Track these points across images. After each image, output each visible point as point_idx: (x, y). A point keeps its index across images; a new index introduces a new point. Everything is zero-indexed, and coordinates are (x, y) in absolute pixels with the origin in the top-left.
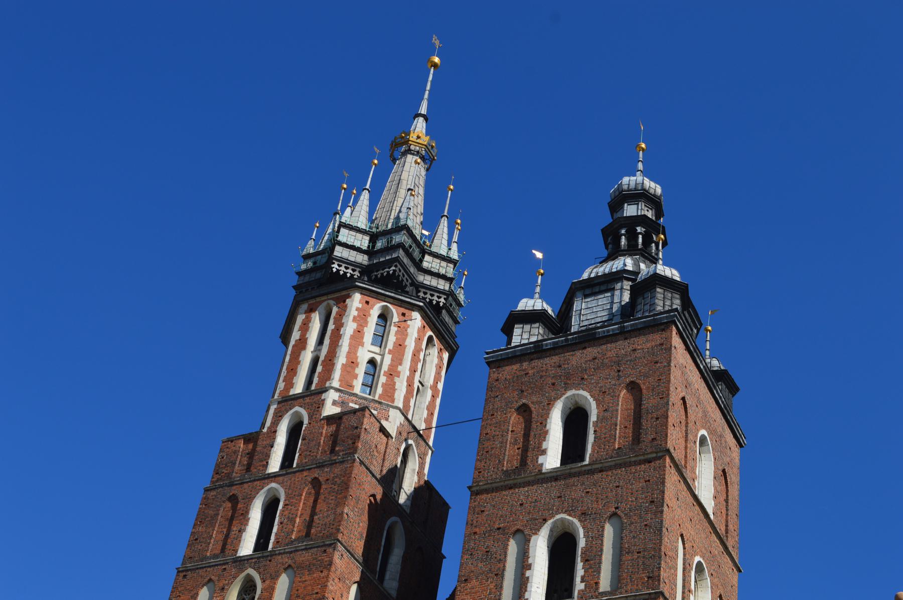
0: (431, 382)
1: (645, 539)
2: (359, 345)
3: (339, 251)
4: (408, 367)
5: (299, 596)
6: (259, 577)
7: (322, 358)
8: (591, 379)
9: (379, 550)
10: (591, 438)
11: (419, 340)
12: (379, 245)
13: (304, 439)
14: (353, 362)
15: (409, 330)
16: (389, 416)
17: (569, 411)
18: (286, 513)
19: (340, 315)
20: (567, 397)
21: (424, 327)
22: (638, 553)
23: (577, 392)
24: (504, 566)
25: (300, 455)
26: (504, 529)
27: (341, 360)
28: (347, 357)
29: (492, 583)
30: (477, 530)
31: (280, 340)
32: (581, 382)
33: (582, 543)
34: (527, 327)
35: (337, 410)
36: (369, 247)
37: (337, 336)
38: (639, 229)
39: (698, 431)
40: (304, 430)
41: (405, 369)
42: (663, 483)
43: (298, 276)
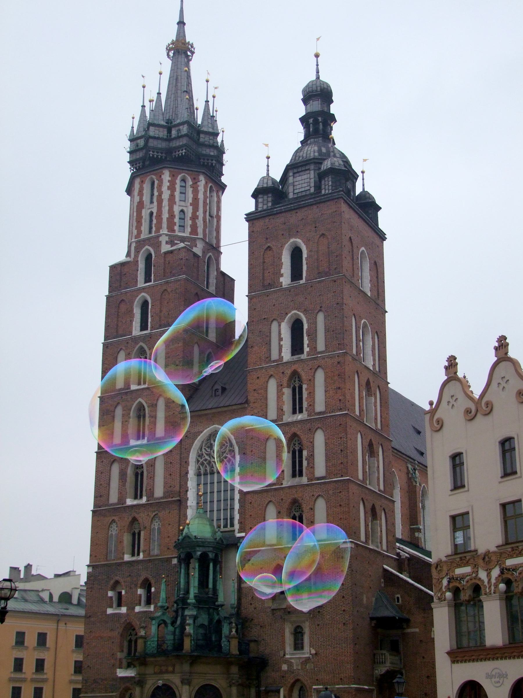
0: (215, 213)
1: (336, 324)
3: (152, 143)
4: (202, 212)
7: (155, 214)
11: (205, 192)
12: (174, 132)
13: (154, 266)
14: (172, 216)
15: (199, 188)
19: (160, 186)
21: (207, 182)
22: (333, 331)
23: (295, 240)
26: (267, 318)
27: (165, 215)
32: (297, 234)
33: (306, 326)
34: (265, 197)
36: (167, 136)
37: (160, 201)
38: (320, 119)
39: (359, 250)
41: (200, 213)
42: (342, 293)
43: (129, 154)
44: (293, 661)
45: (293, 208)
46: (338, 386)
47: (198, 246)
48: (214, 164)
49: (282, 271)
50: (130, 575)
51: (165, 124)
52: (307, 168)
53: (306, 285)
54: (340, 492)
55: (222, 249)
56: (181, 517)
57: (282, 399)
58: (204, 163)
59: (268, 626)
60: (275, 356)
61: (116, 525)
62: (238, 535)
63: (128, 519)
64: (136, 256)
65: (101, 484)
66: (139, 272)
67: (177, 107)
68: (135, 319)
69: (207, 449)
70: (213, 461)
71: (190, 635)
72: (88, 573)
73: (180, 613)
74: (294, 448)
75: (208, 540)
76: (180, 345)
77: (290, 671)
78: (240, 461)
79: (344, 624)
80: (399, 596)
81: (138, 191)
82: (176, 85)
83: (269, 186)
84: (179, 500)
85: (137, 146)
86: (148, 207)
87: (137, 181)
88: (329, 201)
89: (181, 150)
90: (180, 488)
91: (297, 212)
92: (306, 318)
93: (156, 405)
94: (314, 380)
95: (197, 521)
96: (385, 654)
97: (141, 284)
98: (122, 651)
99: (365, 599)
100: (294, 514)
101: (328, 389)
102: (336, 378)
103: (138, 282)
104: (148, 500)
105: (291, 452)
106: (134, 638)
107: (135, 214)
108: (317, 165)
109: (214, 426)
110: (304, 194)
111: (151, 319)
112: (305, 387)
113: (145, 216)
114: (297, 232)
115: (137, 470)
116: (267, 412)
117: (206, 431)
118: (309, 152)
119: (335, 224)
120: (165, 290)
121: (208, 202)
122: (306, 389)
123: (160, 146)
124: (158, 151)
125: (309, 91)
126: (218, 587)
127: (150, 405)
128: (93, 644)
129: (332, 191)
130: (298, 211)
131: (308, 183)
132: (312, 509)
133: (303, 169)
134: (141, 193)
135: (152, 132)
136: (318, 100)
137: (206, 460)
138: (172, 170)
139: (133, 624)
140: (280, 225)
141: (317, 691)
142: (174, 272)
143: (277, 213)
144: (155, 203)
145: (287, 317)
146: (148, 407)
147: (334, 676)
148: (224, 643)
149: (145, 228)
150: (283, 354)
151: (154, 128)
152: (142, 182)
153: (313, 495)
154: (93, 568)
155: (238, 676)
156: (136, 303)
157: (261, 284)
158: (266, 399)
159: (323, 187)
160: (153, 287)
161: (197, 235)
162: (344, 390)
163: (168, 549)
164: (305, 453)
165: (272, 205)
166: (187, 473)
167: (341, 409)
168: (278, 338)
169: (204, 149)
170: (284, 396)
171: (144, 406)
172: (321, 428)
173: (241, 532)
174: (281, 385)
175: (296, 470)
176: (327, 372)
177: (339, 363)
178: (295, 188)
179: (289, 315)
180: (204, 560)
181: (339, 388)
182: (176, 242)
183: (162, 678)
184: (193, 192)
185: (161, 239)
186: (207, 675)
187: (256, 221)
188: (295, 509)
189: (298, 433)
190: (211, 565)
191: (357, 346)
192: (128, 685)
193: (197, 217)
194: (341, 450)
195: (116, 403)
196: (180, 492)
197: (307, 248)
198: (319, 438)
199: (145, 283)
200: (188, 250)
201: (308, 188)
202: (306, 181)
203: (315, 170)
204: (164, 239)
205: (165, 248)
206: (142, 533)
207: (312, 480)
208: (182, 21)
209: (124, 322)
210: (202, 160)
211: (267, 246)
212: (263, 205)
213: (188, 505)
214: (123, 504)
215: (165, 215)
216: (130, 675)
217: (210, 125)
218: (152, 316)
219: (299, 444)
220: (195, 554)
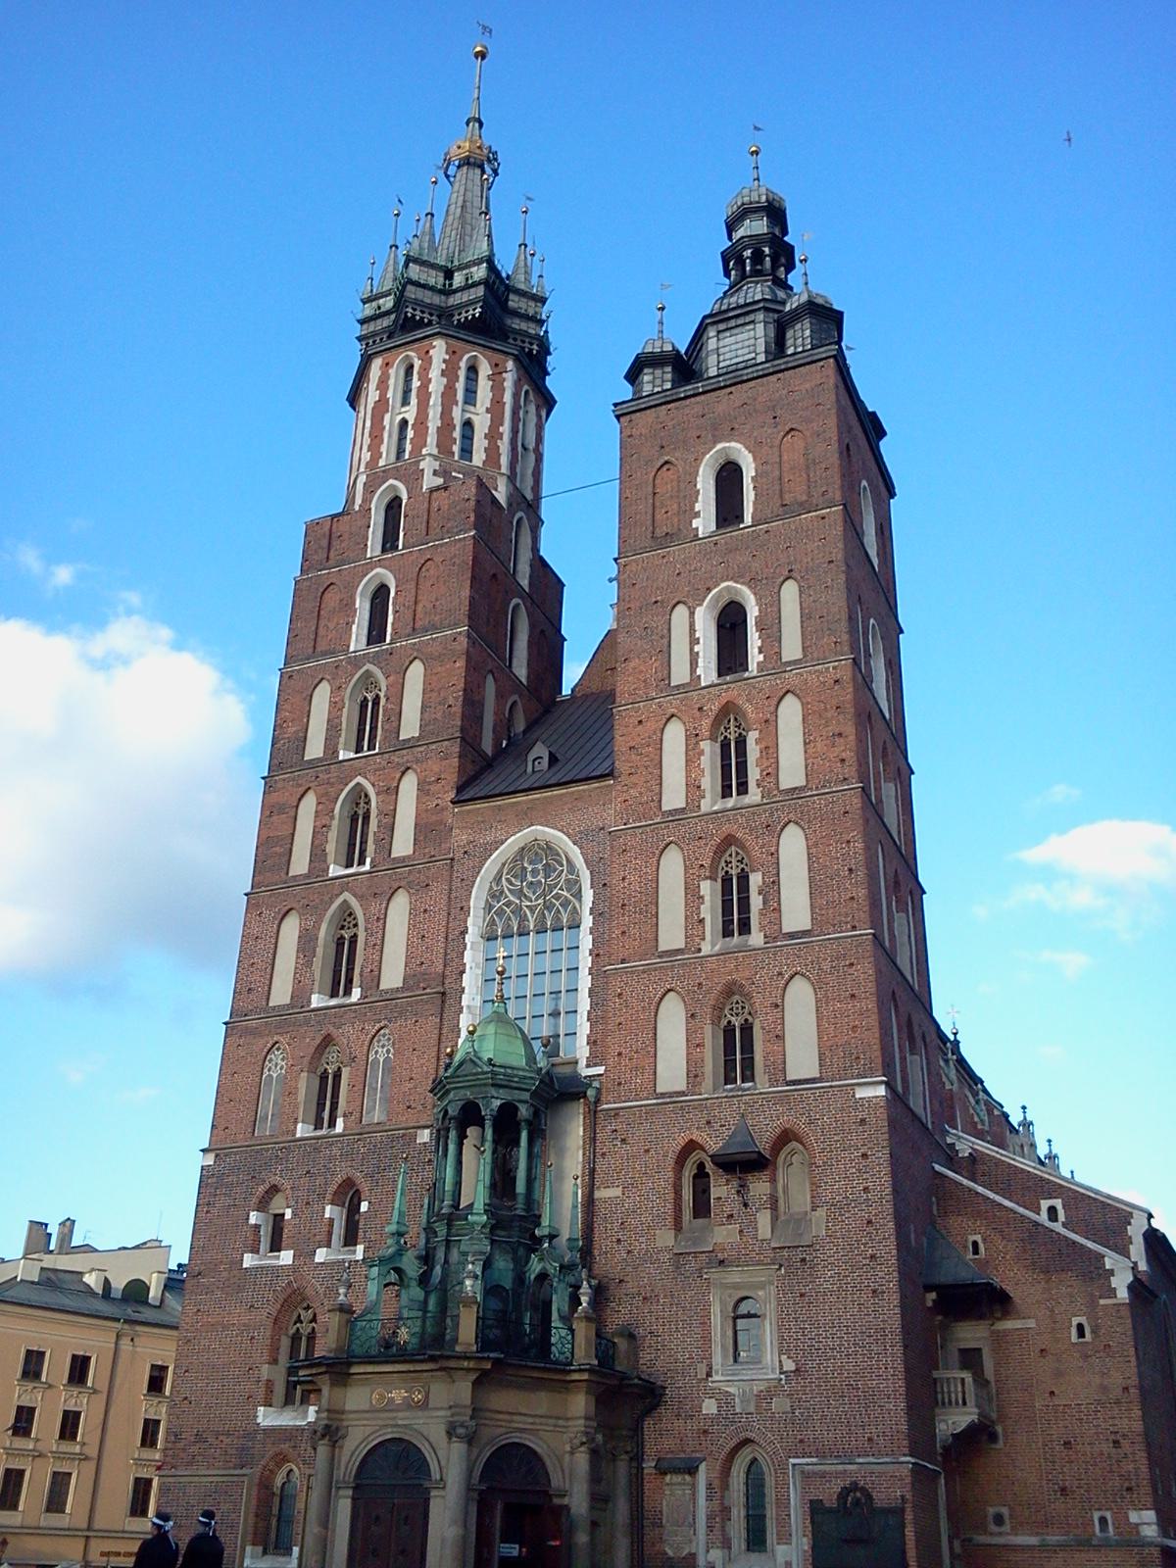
1: (827, 602)
3: (412, 292)
7: (411, 423)
8: (743, 429)
12: (458, 279)
13: (405, 517)
21: (520, 380)
23: (727, 445)
24: (669, 642)
25: (405, 535)
26: (662, 602)
30: (632, 606)
31: (347, 404)
32: (732, 433)
33: (753, 612)
34: (658, 372)
35: (440, 481)
36: (444, 285)
38: (767, 250)
44: (731, 1390)
45: (722, 384)
46: (837, 732)
47: (499, 489)
48: (535, 352)
49: (698, 507)
50: (308, 1172)
52: (748, 319)
54: (852, 964)
55: (546, 510)
56: (444, 1031)
57: (699, 764)
59: (665, 1297)
60: (680, 674)
61: (281, 1056)
62: (586, 1072)
63: (312, 1041)
64: (367, 500)
65: (253, 964)
67: (464, 250)
69: (513, 880)
70: (527, 906)
71: (469, 1302)
72: (203, 1168)
73: (440, 1255)
74: (727, 872)
75: (521, 1073)
76: (458, 664)
77: (727, 1413)
78: (593, 902)
79: (874, 1291)
80: (978, 1238)
84: (443, 994)
85: (379, 308)
87: (377, 364)
90: (445, 966)
91: (731, 393)
92: (755, 594)
94: (776, 721)
95: (491, 1029)
96: (963, 1380)
98: (274, 1361)
99: (913, 1236)
100: (729, 1022)
101: (811, 738)
104: (363, 997)
105: (719, 880)
106: (305, 1330)
107: (368, 424)
108: (771, 315)
109: (533, 828)
111: (394, 618)
112: (752, 737)
114: (732, 429)
115: (343, 932)
117: (513, 838)
120: (429, 559)
122: (757, 742)
124: (424, 309)
126: (536, 1195)
127: (381, 789)
128: (203, 1342)
130: (732, 389)
131: (752, 348)
132: (777, 1006)
133: (740, 321)
134: (383, 384)
135: (414, 272)
136: (762, 219)
137: (508, 904)
138: (451, 341)
139: (309, 1292)
140: (692, 420)
141: (803, 1472)
143: (686, 398)
144: (414, 400)
145: (710, 596)
146: (378, 794)
147: (850, 1432)
148: (558, 1333)
149: (388, 448)
153: (780, 974)
154: (216, 1156)
155: (595, 1425)
157: (649, 535)
159: (789, 342)
160: (402, 555)
163: (409, 1107)
164: (756, 880)
166: (464, 932)
167: (845, 779)
169: (517, 321)
170: (702, 758)
171: (366, 796)
172: (797, 823)
173: (595, 1065)
175: (733, 920)
176: (808, 703)
177: (836, 681)
179: (714, 592)
180: (506, 1125)
181: (840, 735)
183: (391, 1423)
185: (422, 465)
186: (515, 1418)
187: (638, 414)
188: (732, 1009)
189: (739, 835)
190: (524, 1135)
192: (285, 1447)
194: (850, 870)
195: (301, 790)
196: (444, 976)
197: (755, 459)
198: (793, 845)
201: (753, 355)
202: (747, 343)
203: (766, 323)
204: (428, 465)
205: (429, 481)
206: (345, 1073)
207: (775, 939)
208: (477, 116)
211: (662, 461)
212: (654, 387)
213: (464, 1003)
214: (302, 1007)
215: (434, 422)
216: (291, 1423)
218: (396, 612)
219: (738, 861)
220: (487, 1106)
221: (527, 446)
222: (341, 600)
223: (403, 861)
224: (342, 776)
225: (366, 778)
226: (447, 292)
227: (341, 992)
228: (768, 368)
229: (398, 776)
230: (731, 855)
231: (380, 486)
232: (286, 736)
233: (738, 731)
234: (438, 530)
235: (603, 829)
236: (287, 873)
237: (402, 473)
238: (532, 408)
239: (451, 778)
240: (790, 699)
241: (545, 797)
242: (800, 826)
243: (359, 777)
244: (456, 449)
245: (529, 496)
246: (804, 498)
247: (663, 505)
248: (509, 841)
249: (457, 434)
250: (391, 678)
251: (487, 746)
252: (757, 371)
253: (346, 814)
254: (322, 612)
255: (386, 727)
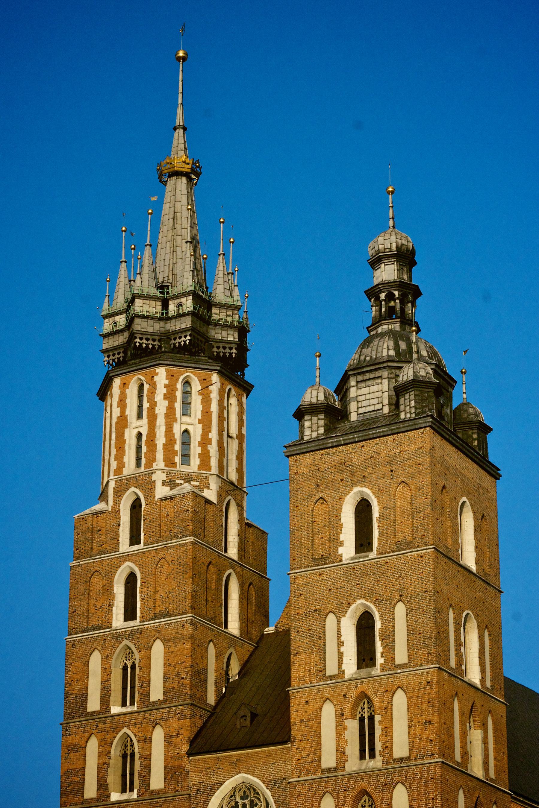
2: (173, 422)
3: (139, 325)
5: (171, 665)
6: (135, 647)
7: (144, 438)
9: (222, 604)
10: (376, 533)
12: (172, 307)
13: (144, 520)
16: (209, 484)
17: (357, 503)
18: (145, 590)
20: (355, 493)
23: (361, 489)
25: (145, 535)
26: (320, 611)
27: (161, 440)
28: (166, 436)
29: (316, 656)
30: (299, 611)
33: (378, 625)
34: (315, 419)
36: (162, 314)
38: (396, 293)
39: (458, 503)
40: (143, 511)
45: (357, 440)
47: (211, 487)
48: (234, 355)
49: (342, 537)
51: (158, 294)
52: (378, 374)
53: (378, 560)
58: (218, 353)
60: (331, 669)
64: (117, 503)
66: (121, 528)
68: (115, 602)
76: (186, 646)
81: (117, 400)
82: (174, 228)
83: (320, 402)
86: (134, 425)
87: (117, 382)
88: (411, 430)
89: (183, 336)
91: (363, 446)
93: (151, 738)
94: (392, 709)
97: (124, 546)
102: (424, 706)
103: (120, 545)
107: (114, 436)
108: (393, 371)
109: (241, 775)
110: (373, 415)
112: (377, 718)
113: (130, 439)
114: (364, 476)
116: (320, 756)
117: (228, 782)
118: (380, 349)
119: (421, 467)
121: (226, 416)
122: (380, 723)
123: (150, 330)
125: (379, 250)
129: (416, 415)
130: (364, 443)
133: (372, 376)
135: (140, 306)
136: (394, 264)
138: (169, 368)
142: (175, 531)
144: (145, 420)
145: (350, 609)
146: (139, 742)
150: (344, 667)
151: (141, 301)
152: (124, 385)
156: (116, 577)
157: (310, 557)
158: (319, 735)
159: (402, 408)
161: (210, 469)
162: (436, 725)
165: (325, 431)
168: (336, 641)
172: (403, 784)
174: (343, 715)
177: (428, 683)
178: (360, 406)
179: (353, 606)
181: (430, 722)
182: (178, 481)
184: (202, 401)
185: (154, 477)
191: (457, 655)
193: (210, 442)
195: (87, 735)
197: (379, 503)
199: (130, 545)
200: (196, 495)
201: (379, 406)
202: (377, 395)
204: (159, 477)
205: (161, 491)
209: (99, 605)
210: (215, 350)
211: (318, 497)
212: (312, 431)
215: (161, 440)
217: (228, 293)
221: (231, 435)
222: (103, 586)
223: (156, 793)
224: (114, 726)
225: (130, 730)
226: (165, 318)
227: (128, 790)
228: (387, 431)
229: (151, 729)
230: (365, 801)
231: (125, 492)
232: (74, 692)
233: (370, 712)
234: (168, 533)
235: (284, 779)
236: (83, 797)
237: (140, 482)
238: (233, 401)
239: (187, 734)
240: (400, 692)
241: (248, 754)
242: (405, 786)
243: (125, 728)
244: (178, 459)
245: (233, 477)
246: (410, 538)
247: (319, 532)
248: (226, 783)
249: (178, 447)
250: (142, 653)
251: (212, 699)
252: (379, 432)
253: (118, 754)
254: (91, 594)
255: (141, 691)
